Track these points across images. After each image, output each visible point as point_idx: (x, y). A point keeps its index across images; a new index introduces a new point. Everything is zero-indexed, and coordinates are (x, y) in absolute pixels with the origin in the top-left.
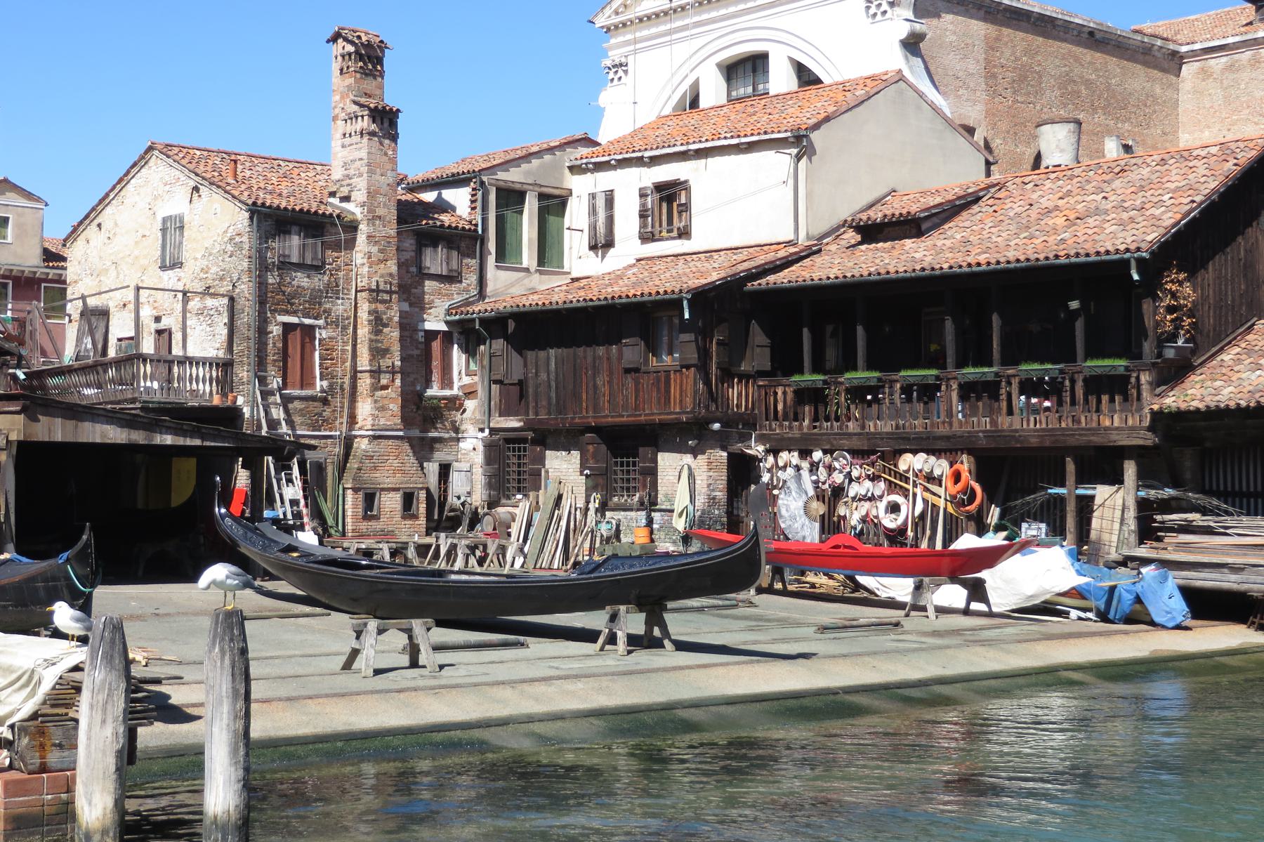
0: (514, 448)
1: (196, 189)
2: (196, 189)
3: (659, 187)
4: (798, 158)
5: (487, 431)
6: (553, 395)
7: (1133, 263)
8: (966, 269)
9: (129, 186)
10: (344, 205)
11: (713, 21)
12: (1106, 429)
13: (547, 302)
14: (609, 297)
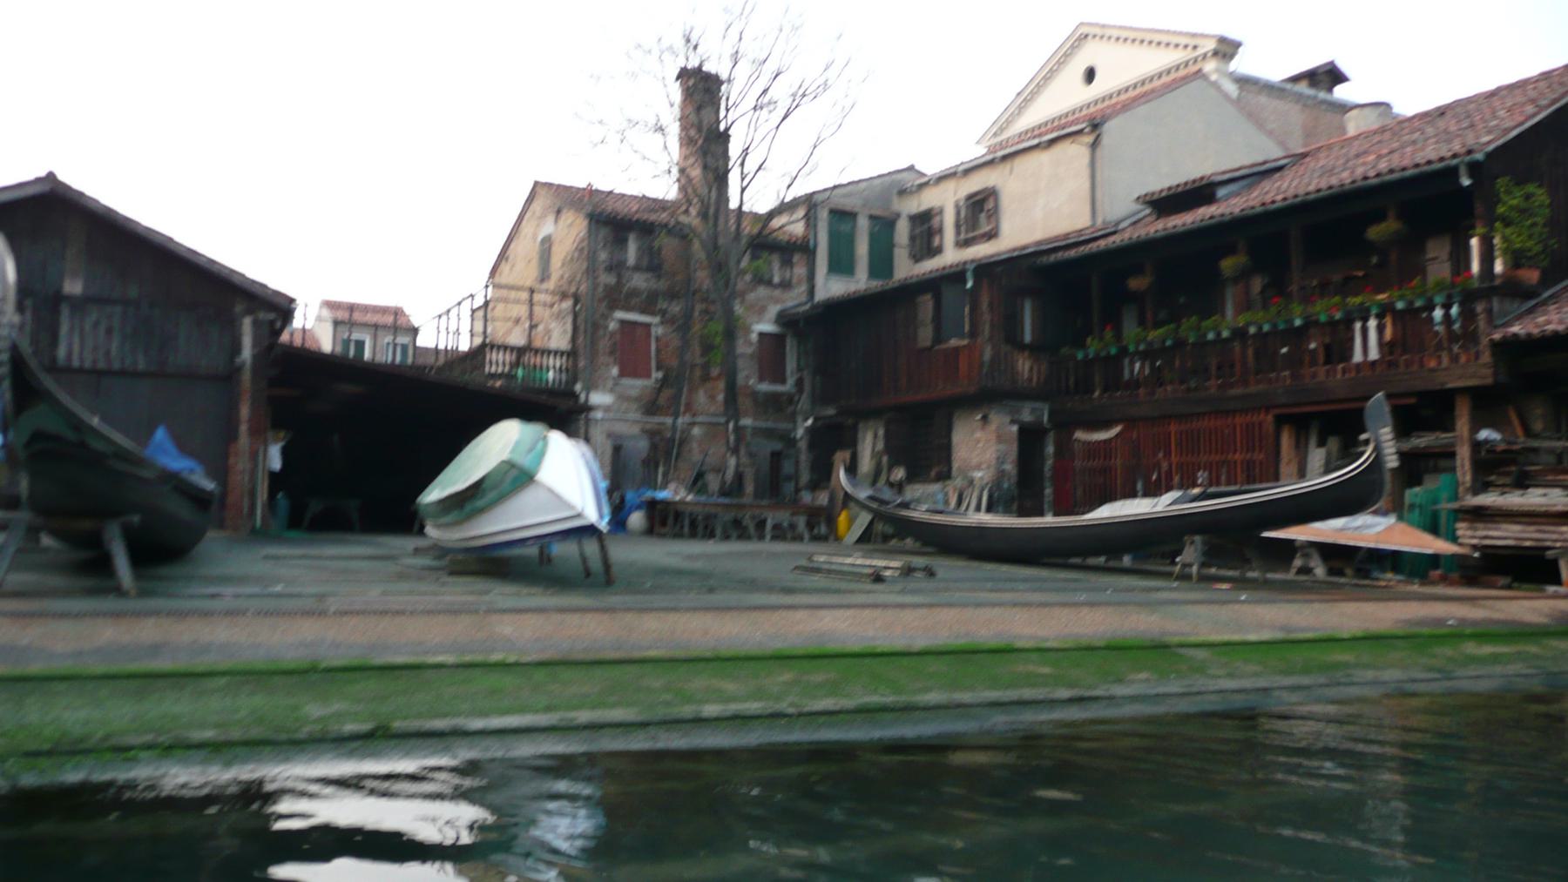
4: (1094, 145)
7: (1463, 171)
12: (1433, 370)
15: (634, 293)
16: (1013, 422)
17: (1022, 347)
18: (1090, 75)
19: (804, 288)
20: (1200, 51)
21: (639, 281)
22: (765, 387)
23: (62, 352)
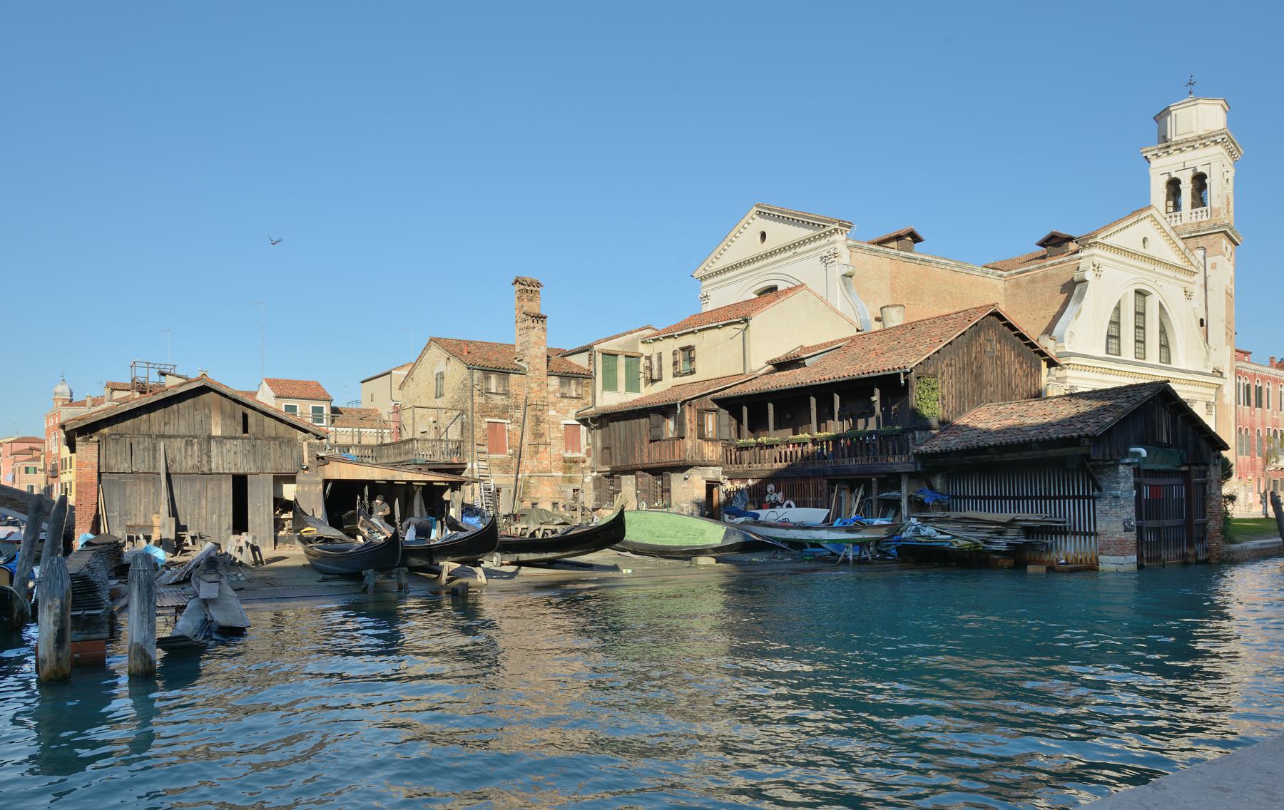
1: (449, 359)
2: (449, 359)
3: (683, 349)
8: (818, 383)
9: (424, 360)
10: (519, 363)
11: (751, 271)
12: (891, 464)
15: (496, 407)
16: (703, 478)
17: (707, 440)
18: (763, 236)
19: (590, 399)
20: (827, 229)
21: (498, 400)
22: (569, 455)
23: (213, 466)
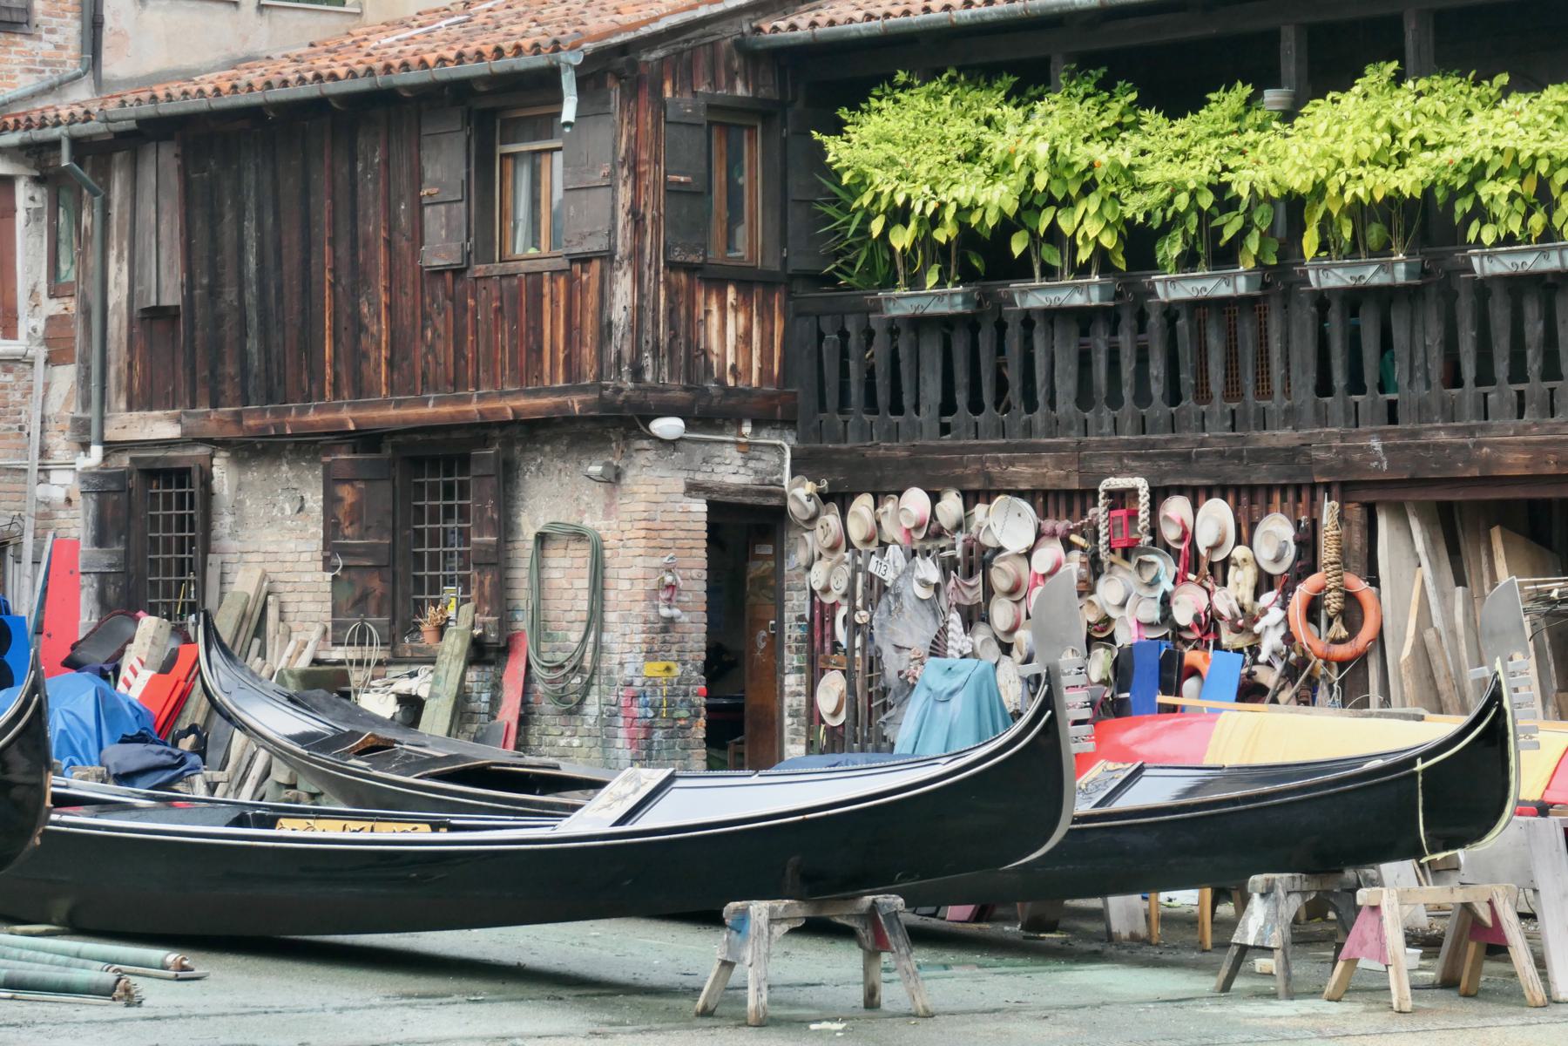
0: (167, 497)
5: (96, 451)
6: (253, 345)
13: (226, 86)
14: (378, 66)
16: (693, 489)
19: (70, 30)
